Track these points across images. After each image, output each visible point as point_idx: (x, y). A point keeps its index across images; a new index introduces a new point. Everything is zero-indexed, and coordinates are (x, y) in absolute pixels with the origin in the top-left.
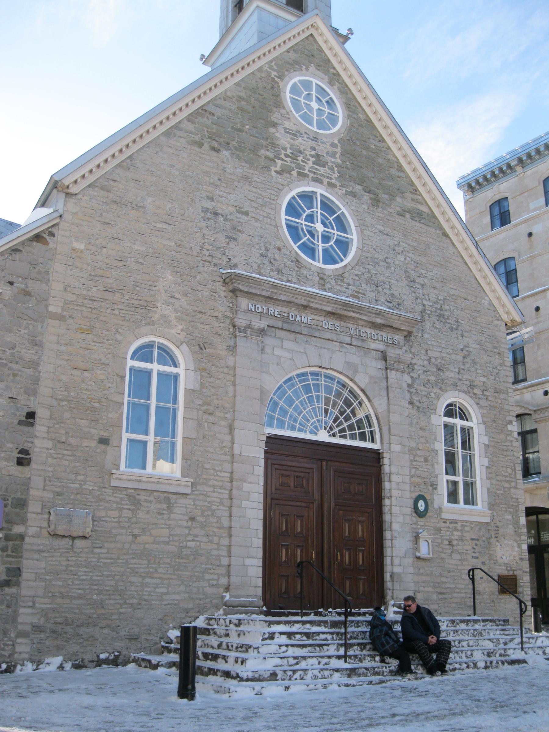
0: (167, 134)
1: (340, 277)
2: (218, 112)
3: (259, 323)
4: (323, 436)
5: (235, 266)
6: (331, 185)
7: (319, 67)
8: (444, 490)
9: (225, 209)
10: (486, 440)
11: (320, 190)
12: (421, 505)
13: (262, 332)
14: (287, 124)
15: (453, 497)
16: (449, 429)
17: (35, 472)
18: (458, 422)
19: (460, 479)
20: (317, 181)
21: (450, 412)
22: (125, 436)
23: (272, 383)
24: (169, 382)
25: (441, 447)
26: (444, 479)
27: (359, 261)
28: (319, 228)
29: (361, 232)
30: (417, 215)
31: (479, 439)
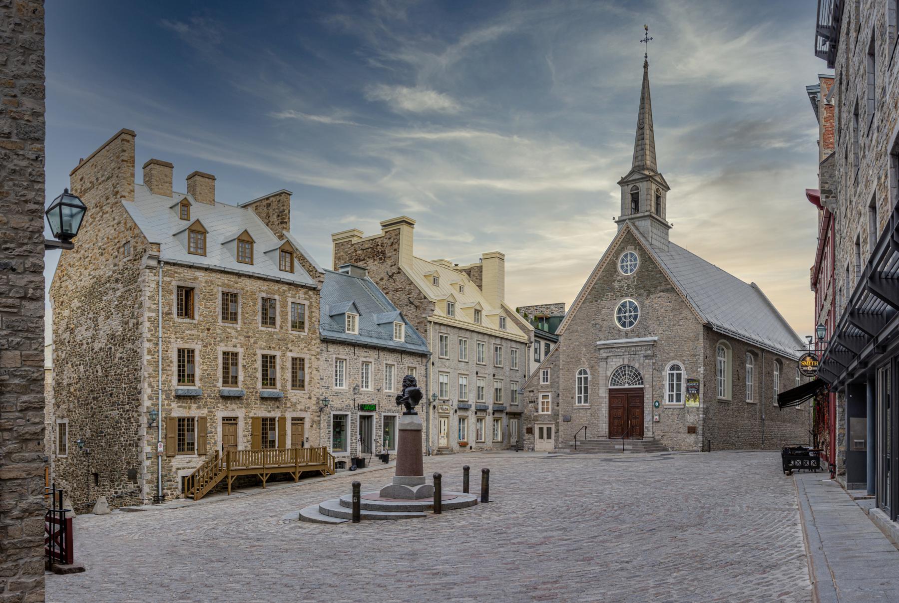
0: (583, 303)
1: (633, 330)
2: (596, 286)
3: (604, 355)
4: (627, 386)
5: (600, 340)
6: (632, 295)
7: (631, 244)
8: (667, 397)
9: (597, 322)
10: (686, 377)
11: (627, 299)
12: (657, 404)
13: (607, 358)
14: (619, 278)
15: (671, 400)
16: (672, 375)
17: (560, 408)
18: (675, 372)
19: (674, 393)
20: (627, 296)
21: (672, 368)
22: (577, 395)
23: (609, 373)
24: (586, 378)
25: (667, 383)
26: (667, 394)
27: (640, 322)
28: (627, 314)
29: (642, 310)
30: (667, 291)
31: (684, 376)
